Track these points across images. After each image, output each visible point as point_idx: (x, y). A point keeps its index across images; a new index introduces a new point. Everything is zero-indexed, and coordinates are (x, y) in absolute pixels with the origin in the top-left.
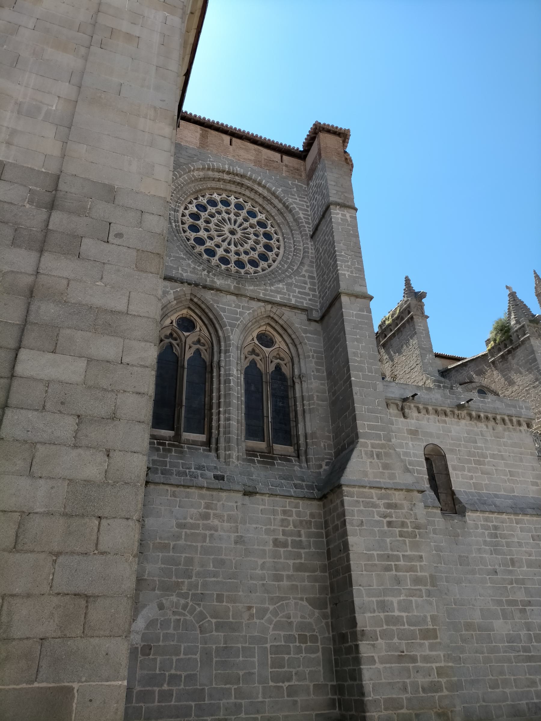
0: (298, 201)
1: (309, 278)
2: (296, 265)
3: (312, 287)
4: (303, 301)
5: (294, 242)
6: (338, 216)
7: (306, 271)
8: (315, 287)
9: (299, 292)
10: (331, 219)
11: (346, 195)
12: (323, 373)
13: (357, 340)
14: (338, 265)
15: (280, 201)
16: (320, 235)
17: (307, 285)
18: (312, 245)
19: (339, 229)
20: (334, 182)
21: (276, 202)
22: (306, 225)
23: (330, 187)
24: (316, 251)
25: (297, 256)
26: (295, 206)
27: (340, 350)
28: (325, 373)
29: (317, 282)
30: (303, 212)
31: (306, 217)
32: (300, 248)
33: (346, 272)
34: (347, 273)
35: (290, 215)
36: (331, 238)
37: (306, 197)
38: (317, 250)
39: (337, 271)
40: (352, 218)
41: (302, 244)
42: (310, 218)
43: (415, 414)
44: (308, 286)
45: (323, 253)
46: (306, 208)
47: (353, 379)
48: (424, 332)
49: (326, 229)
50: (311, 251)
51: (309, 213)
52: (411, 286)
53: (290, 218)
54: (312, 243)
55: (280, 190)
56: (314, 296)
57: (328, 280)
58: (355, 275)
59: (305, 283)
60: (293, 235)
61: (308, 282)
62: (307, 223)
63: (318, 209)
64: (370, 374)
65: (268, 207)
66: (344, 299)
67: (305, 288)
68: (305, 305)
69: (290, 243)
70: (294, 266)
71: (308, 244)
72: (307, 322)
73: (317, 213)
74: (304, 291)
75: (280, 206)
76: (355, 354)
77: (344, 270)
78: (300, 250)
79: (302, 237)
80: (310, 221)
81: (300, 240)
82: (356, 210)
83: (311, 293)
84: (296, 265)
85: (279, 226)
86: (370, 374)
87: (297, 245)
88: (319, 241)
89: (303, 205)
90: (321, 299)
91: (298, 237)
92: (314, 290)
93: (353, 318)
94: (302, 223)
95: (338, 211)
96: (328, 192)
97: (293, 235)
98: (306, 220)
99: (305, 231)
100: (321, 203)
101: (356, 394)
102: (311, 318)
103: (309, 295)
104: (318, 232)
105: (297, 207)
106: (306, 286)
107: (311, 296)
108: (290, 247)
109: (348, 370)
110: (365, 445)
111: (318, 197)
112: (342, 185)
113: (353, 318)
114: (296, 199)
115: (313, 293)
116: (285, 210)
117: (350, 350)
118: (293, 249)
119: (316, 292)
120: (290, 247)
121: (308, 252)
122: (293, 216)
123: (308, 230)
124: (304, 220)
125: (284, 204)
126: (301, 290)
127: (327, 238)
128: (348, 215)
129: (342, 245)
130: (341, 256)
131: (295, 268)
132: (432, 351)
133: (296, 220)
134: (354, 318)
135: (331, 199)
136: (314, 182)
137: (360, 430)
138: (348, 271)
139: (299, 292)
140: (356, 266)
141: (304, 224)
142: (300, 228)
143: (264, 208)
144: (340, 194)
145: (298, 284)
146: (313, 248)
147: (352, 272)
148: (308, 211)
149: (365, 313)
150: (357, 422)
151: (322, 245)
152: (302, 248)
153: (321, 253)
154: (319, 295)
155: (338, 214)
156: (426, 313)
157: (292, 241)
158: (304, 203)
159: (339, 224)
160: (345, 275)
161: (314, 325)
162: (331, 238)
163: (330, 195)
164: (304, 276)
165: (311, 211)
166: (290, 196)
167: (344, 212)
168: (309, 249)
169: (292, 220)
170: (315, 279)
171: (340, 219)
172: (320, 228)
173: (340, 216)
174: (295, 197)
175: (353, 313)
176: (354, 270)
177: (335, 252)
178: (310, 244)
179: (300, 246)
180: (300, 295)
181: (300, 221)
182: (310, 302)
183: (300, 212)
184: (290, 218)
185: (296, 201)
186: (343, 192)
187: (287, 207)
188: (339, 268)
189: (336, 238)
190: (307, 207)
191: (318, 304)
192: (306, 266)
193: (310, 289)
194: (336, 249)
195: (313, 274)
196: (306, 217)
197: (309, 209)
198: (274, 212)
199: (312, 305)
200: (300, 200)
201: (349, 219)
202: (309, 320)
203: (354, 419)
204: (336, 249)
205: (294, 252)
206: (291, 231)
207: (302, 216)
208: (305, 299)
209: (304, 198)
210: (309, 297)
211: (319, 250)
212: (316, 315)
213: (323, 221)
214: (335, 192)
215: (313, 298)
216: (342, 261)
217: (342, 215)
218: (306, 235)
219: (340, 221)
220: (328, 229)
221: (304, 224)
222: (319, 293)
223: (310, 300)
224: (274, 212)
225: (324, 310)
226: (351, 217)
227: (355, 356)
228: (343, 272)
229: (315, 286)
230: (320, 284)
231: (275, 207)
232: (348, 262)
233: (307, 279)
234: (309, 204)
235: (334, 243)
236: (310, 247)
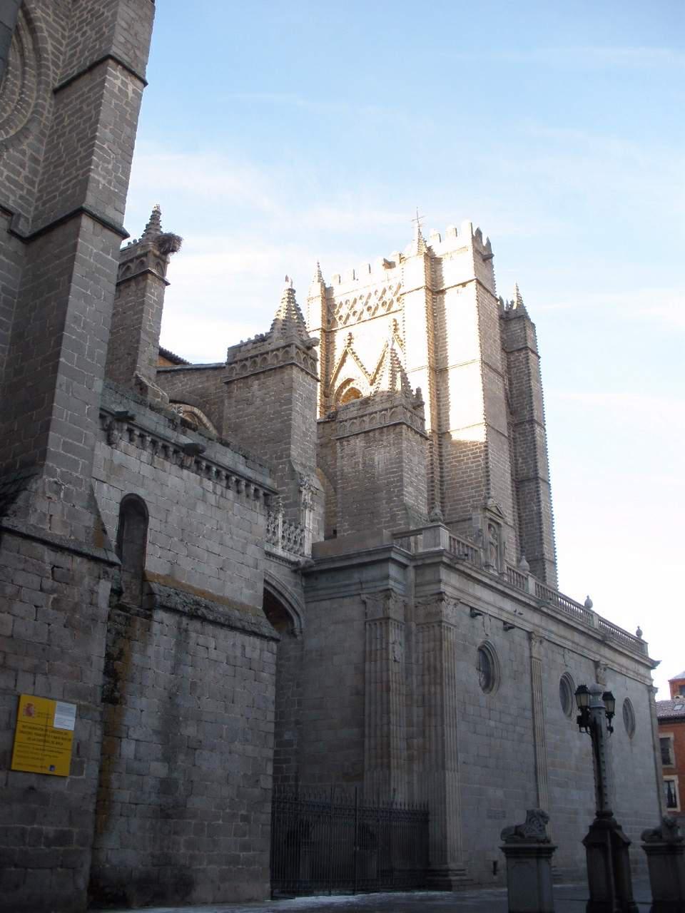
0: (51, 20)
1: (30, 159)
2: (14, 127)
3: (30, 176)
4: (11, 196)
5: (23, 85)
6: (116, 81)
7: (28, 145)
8: (35, 179)
9: (8, 178)
10: (104, 81)
11: (138, 53)
12: (7, 330)
13: (85, 296)
14: (93, 163)
16: (73, 94)
17: (24, 169)
18: (51, 106)
19: (111, 103)
20: (127, 23)
22: (52, 67)
23: (118, 29)
24: (56, 118)
25: (22, 113)
26: (44, 26)
27: (52, 303)
28: (10, 332)
29: (41, 171)
30: (55, 44)
31: (57, 53)
32: (30, 101)
33: (101, 179)
34: (103, 182)
35: (29, 37)
36: (93, 112)
37: (66, 20)
38: (59, 119)
39: (89, 170)
40: (136, 95)
41: (35, 95)
42: (62, 58)
43: (124, 443)
44: (25, 172)
45: (68, 129)
46: (60, 38)
47: (62, 359)
48: (156, 306)
49: (89, 92)
50: (47, 115)
51: (62, 49)
52: (158, 224)
54: (53, 102)
56: (29, 192)
57: (65, 177)
58: (112, 188)
59: (23, 166)
60: (24, 73)
61: (27, 165)
62: (55, 64)
63: (82, 52)
64: (89, 360)
66: (86, 222)
67: (19, 174)
68: (11, 203)
69: (15, 85)
70: (11, 128)
71: (45, 101)
72: (5, 234)
73: (79, 58)
74: (17, 178)
76: (76, 320)
77: (99, 174)
78: (29, 104)
79: (39, 83)
80: (60, 63)
81: (35, 87)
82: (145, 84)
83: (27, 186)
84: (14, 127)
86: (89, 360)
87: (26, 95)
88: (67, 105)
89: (57, 31)
90: (40, 203)
91: (31, 81)
92: (32, 183)
93: (90, 258)
94: (47, 60)
95: (118, 74)
96: (113, 35)
97: (24, 73)
98: (54, 59)
99: (48, 76)
100: (91, 45)
101: (61, 385)
102: (15, 230)
103: (22, 188)
104: (68, 91)
105: (47, 31)
106: (21, 170)
107: (25, 191)
108: (13, 93)
109: (59, 343)
110: (52, 473)
111: (89, 32)
112: (136, 35)
113: (90, 258)
114: (48, 14)
115: (29, 187)
116: (24, 23)
117: (72, 310)
118: (17, 97)
119: (34, 188)
120: (13, 93)
121: (42, 115)
122: (35, 41)
123: (55, 77)
124: (51, 57)
126: (12, 176)
127: (85, 108)
128: (131, 87)
129: (107, 131)
130: (102, 148)
132: (157, 340)
133: (38, 51)
134: (92, 260)
135: (115, 50)
136: (89, 4)
137: (51, 448)
138: (104, 178)
139: (8, 178)
140: (119, 174)
141: (50, 64)
144: (129, 46)
145: (12, 163)
146: (52, 110)
147: (109, 183)
148: (61, 44)
149: (110, 257)
150: (51, 433)
151: (72, 115)
152: (32, 102)
153: (64, 127)
154: (38, 195)
155: (116, 78)
156: (168, 278)
157: (19, 83)
158: (60, 29)
159: (113, 94)
160: (98, 182)
161: (15, 244)
162: (93, 112)
163: (114, 41)
164: (24, 153)
165: (67, 45)
166: (40, 4)
167: (127, 78)
168: (45, 110)
170: (39, 165)
171: (117, 88)
172: (76, 84)
173: (118, 82)
174: (48, 11)
175: (92, 250)
176: (114, 180)
177: (94, 138)
178: (48, 102)
179: (31, 97)
180: (8, 184)
181: (45, 55)
182: (20, 201)
183: (50, 41)
185: (47, 17)
186: (133, 46)
188: (92, 167)
189: (102, 116)
190: (63, 37)
191: (32, 209)
192: (31, 137)
193: (26, 177)
194: (97, 134)
195: (38, 154)
196: (57, 53)
197: (64, 42)
199: (21, 207)
201: (131, 94)
202: (12, 233)
203: (47, 427)
204: (97, 134)
205: (17, 103)
207: (50, 48)
208: (13, 192)
209: (63, 20)
210: (21, 192)
211: (63, 121)
212: (25, 229)
213: (87, 77)
214: (122, 40)
215: (28, 197)
216: (100, 158)
217: (123, 83)
218: (47, 84)
219: (116, 90)
220: (91, 94)
221: (50, 64)
222: (40, 191)
223: (21, 197)
225: (41, 225)
226: (134, 91)
227: (75, 322)
228: (96, 177)
229: (36, 177)
230: (46, 176)
232: (109, 163)
233: (26, 159)
234: (67, 34)
235: (97, 121)
236: (47, 107)
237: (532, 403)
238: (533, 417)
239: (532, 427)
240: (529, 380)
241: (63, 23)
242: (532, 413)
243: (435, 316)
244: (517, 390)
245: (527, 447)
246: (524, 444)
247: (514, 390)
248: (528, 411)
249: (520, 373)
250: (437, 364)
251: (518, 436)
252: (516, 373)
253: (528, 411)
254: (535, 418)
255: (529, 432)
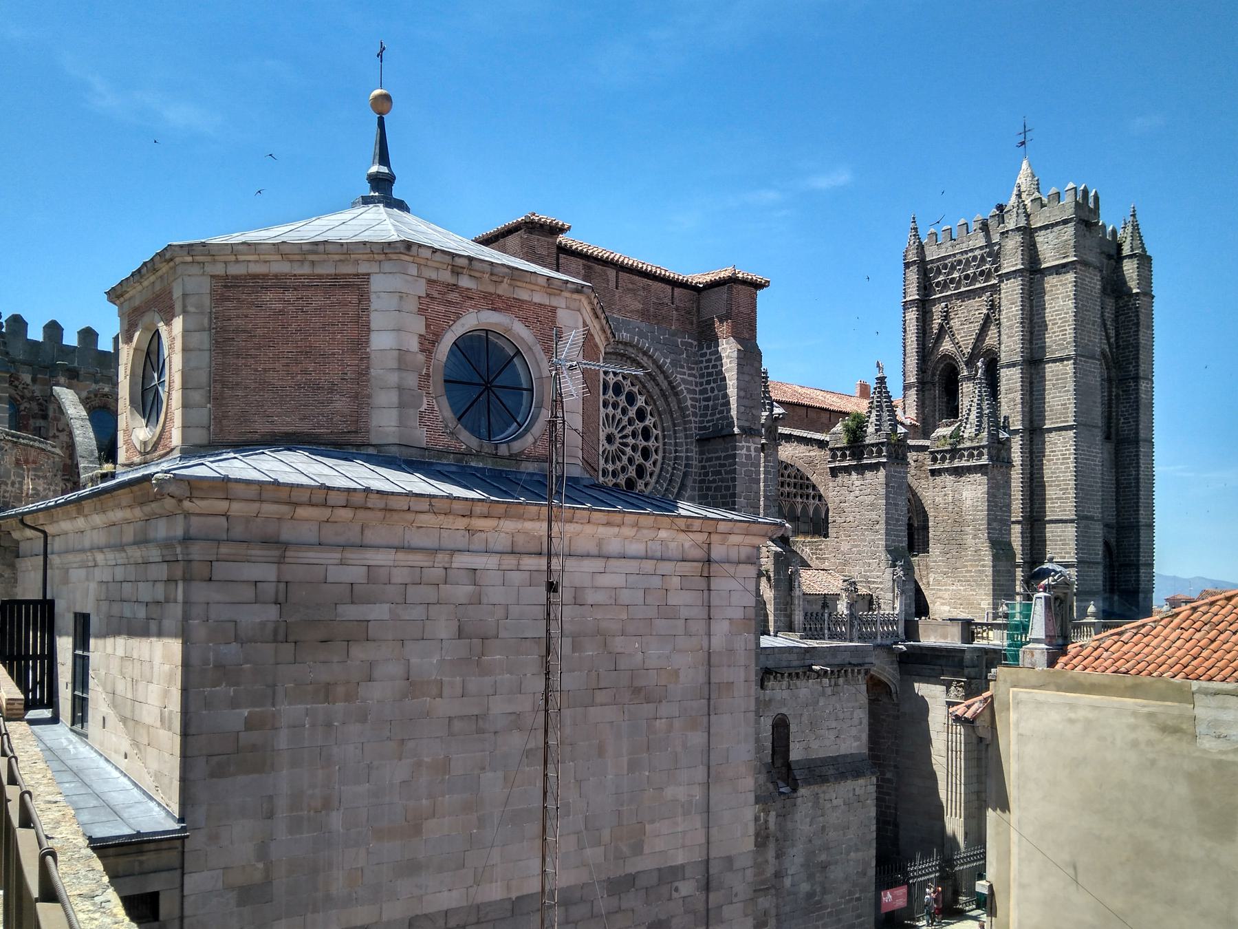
15: (666, 377)
21: (660, 378)
53: (674, 406)
55: (668, 361)
60: (675, 432)
65: (650, 385)
75: (665, 385)
85: (660, 415)
122: (679, 402)
125: (670, 383)
131: (676, 491)
133: (682, 410)
142: (685, 423)
143: (644, 387)
169: (676, 407)
183: (688, 396)
184: (674, 406)
187: (673, 388)
198: (655, 392)
200: (690, 375)
206: (674, 425)
224: (655, 392)
231: (658, 385)
237: (1138, 358)
238: (1137, 374)
239: (1136, 385)
240: (1138, 331)
241: (694, 372)
242: (1137, 370)
243: (1032, 300)
244: (1123, 342)
245: (1130, 406)
246: (1127, 403)
247: (1121, 341)
248: (1134, 367)
249: (1129, 321)
250: (974, 817)
251: (1121, 393)
252: (1124, 322)
253: (1134, 367)
254: (1141, 374)
255: (1133, 390)
